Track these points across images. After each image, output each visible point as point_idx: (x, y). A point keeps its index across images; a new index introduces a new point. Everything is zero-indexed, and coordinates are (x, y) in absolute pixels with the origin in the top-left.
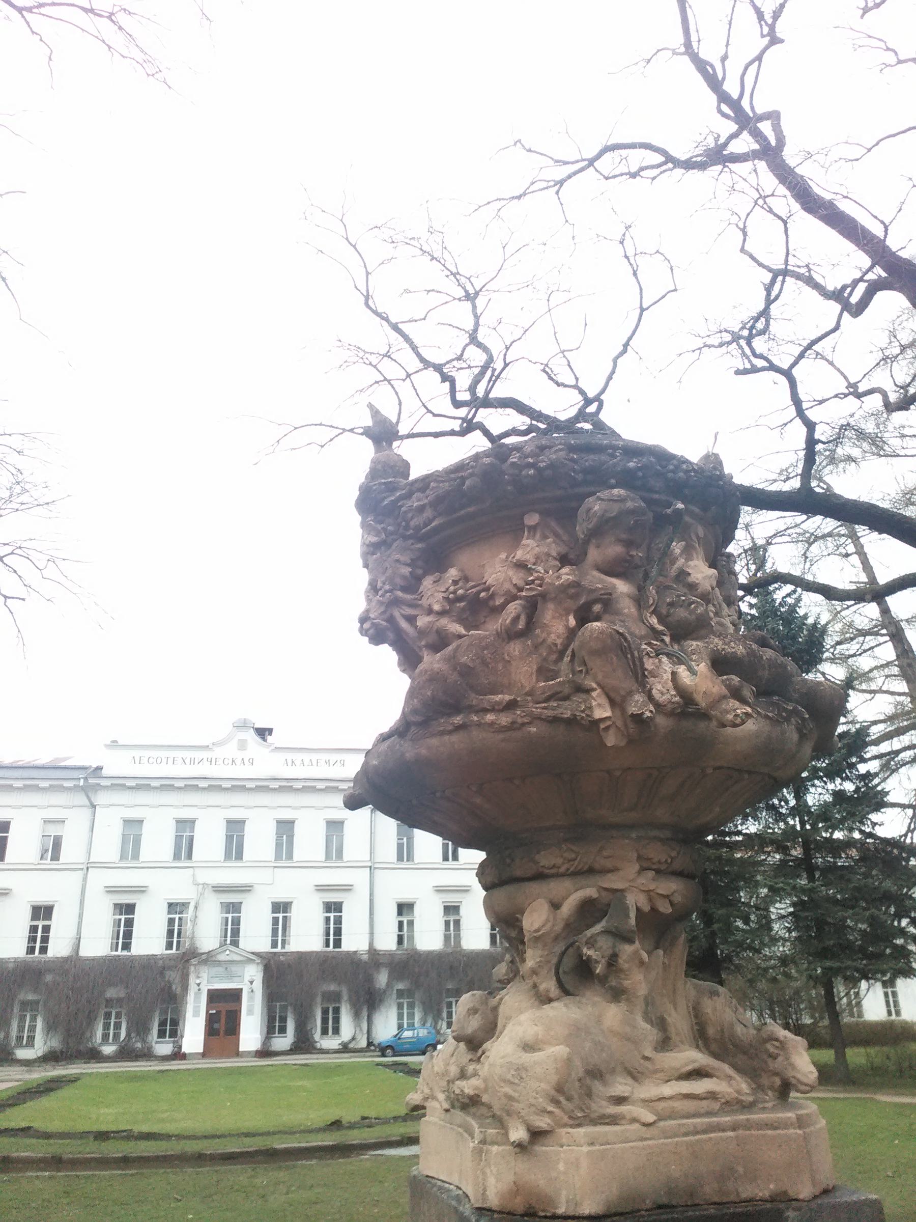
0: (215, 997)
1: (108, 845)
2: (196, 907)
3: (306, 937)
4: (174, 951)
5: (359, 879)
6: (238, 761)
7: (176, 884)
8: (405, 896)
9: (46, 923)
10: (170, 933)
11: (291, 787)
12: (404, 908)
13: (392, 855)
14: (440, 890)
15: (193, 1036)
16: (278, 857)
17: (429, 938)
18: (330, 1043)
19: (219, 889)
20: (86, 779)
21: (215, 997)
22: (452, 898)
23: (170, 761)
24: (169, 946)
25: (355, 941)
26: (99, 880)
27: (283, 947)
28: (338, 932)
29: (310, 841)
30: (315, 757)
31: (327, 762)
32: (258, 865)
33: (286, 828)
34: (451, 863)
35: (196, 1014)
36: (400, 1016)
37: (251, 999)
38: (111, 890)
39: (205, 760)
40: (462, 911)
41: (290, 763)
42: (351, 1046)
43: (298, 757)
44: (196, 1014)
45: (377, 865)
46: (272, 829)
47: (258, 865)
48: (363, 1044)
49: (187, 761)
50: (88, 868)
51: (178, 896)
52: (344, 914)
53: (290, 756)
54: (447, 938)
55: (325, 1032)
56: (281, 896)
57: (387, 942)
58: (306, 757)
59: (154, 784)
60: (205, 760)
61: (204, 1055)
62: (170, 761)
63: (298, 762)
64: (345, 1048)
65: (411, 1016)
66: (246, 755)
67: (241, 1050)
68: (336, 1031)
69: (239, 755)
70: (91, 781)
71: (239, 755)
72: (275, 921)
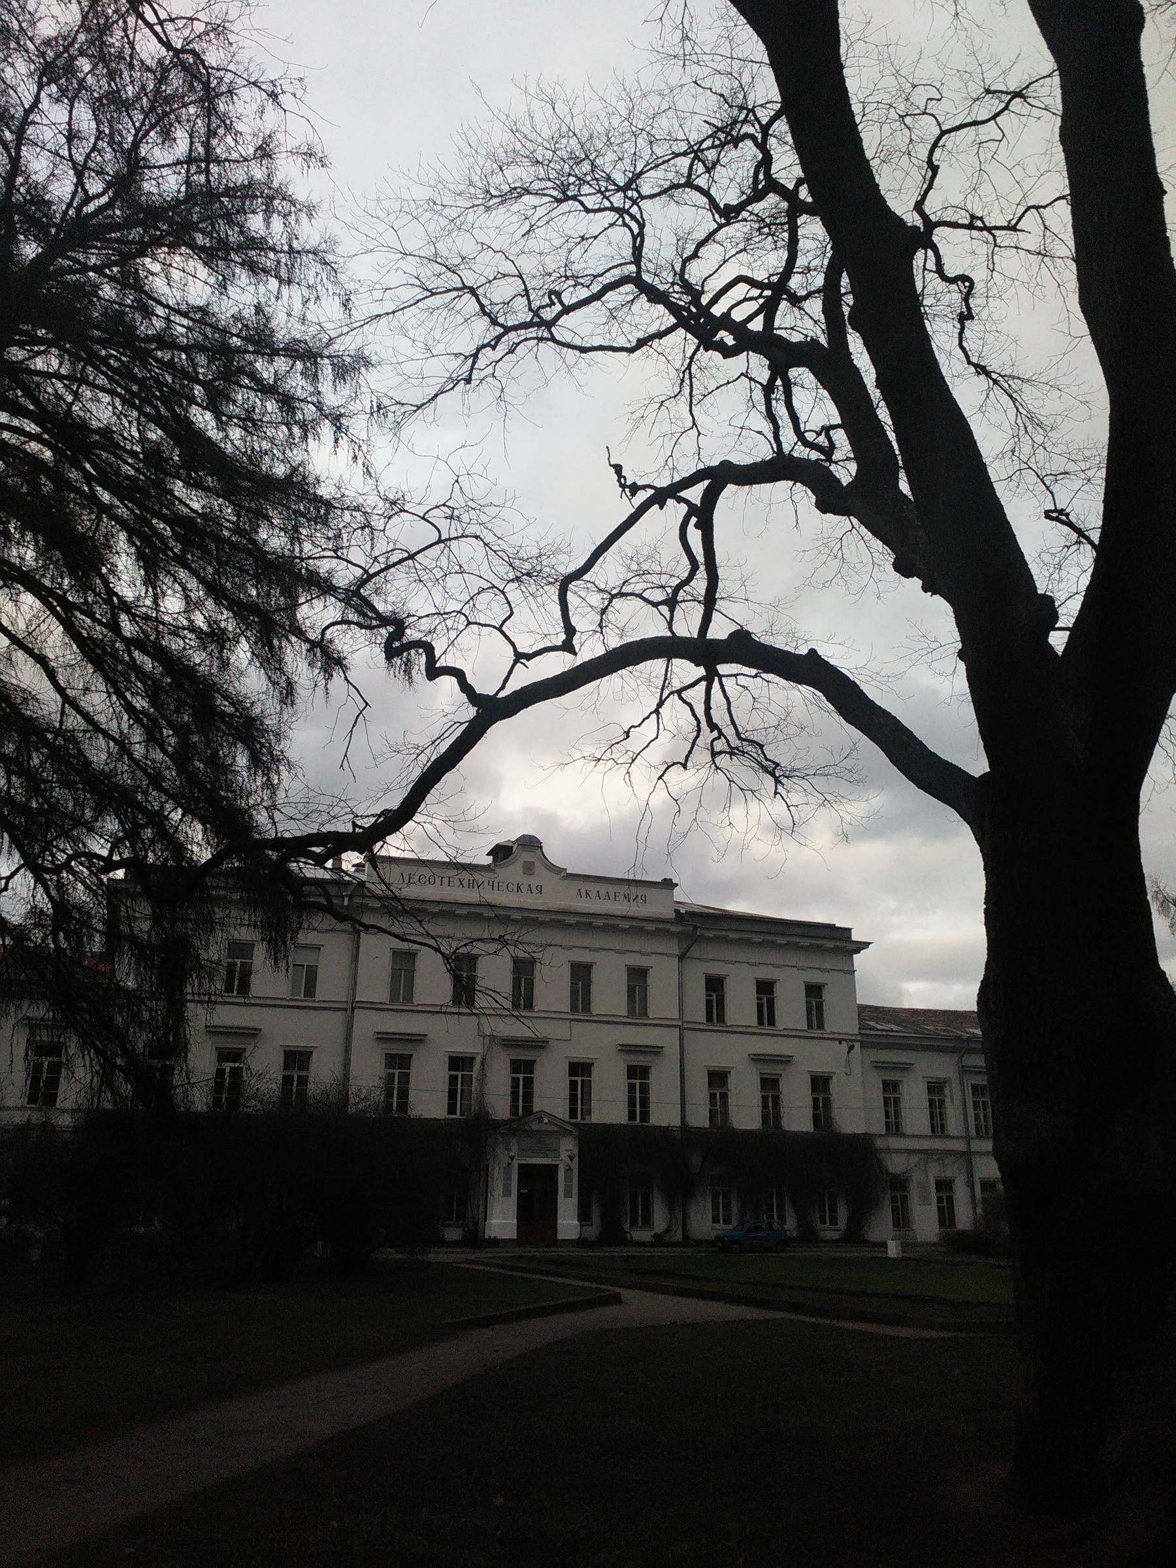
0: (526, 1172)
1: (375, 981)
2: (483, 1064)
3: (608, 1106)
4: (458, 1116)
5: (668, 1039)
6: (524, 888)
7: (456, 1035)
8: (720, 1063)
9: (304, 1073)
10: (631, 1103)
11: (590, 924)
12: (718, 1078)
13: (701, 1016)
14: (757, 1059)
15: (502, 1219)
16: (574, 1008)
17: (746, 1115)
18: (642, 1235)
19: (510, 1043)
20: (350, 897)
21: (526, 1172)
22: (639, 1060)
23: (446, 881)
24: (452, 1109)
25: (664, 1113)
26: (367, 1024)
27: (583, 1118)
28: (645, 1103)
29: (610, 992)
30: (612, 889)
31: (627, 897)
32: (552, 1017)
33: (581, 974)
34: (767, 1029)
35: (507, 1193)
36: (715, 1208)
37: (568, 1178)
38: (383, 1038)
39: (486, 883)
40: (783, 1085)
41: (584, 894)
42: (667, 1238)
43: (593, 888)
44: (568, 1194)
45: (686, 1025)
46: (566, 972)
47: (552, 1017)
48: (679, 1236)
49: (465, 883)
50: (353, 1010)
51: (462, 1048)
52: (413, 1071)
53: (584, 886)
54: (765, 1117)
55: (634, 1222)
56: (580, 1054)
57: (700, 1118)
58: (603, 889)
59: (541, 917)
60: (486, 883)
61: (518, 1242)
62: (446, 881)
63: (593, 894)
64: (658, 1241)
65: (727, 1206)
66: (534, 881)
67: (560, 1237)
68: (647, 1222)
69: (525, 881)
70: (357, 900)
71: (525, 881)
72: (573, 1085)
